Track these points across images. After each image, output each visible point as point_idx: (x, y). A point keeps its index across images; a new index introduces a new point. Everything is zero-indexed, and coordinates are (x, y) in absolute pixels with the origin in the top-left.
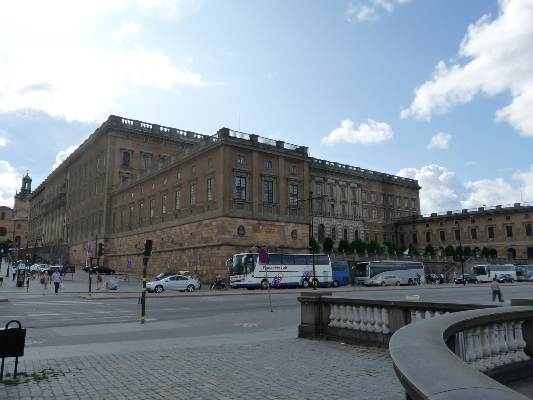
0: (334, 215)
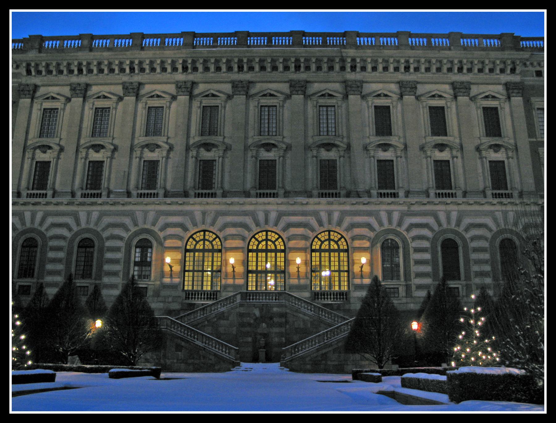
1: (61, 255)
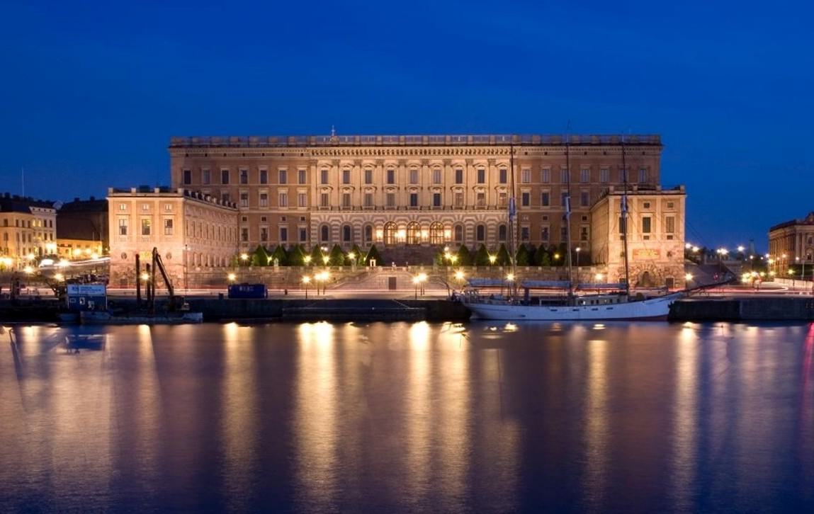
1: (338, 232)
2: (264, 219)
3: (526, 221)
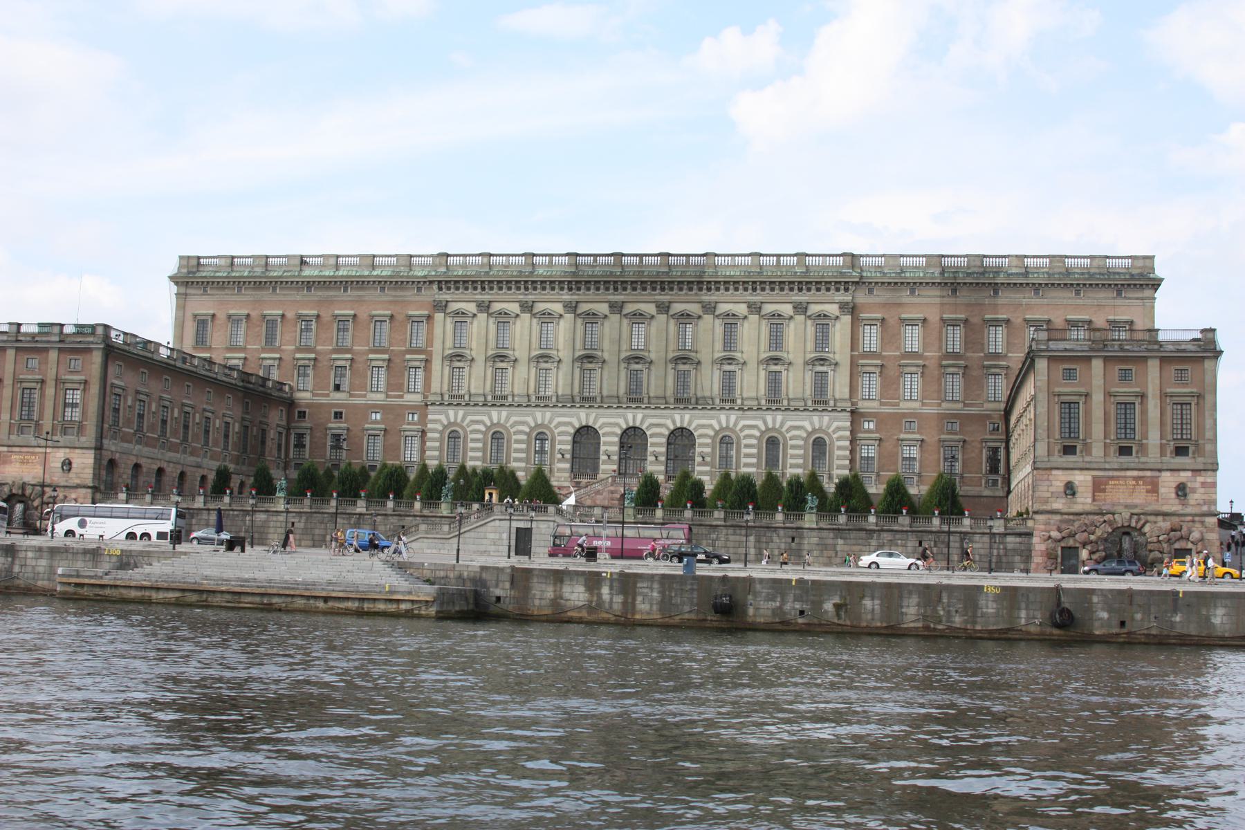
0: (733, 401)
2: (338, 415)
3: (869, 431)
